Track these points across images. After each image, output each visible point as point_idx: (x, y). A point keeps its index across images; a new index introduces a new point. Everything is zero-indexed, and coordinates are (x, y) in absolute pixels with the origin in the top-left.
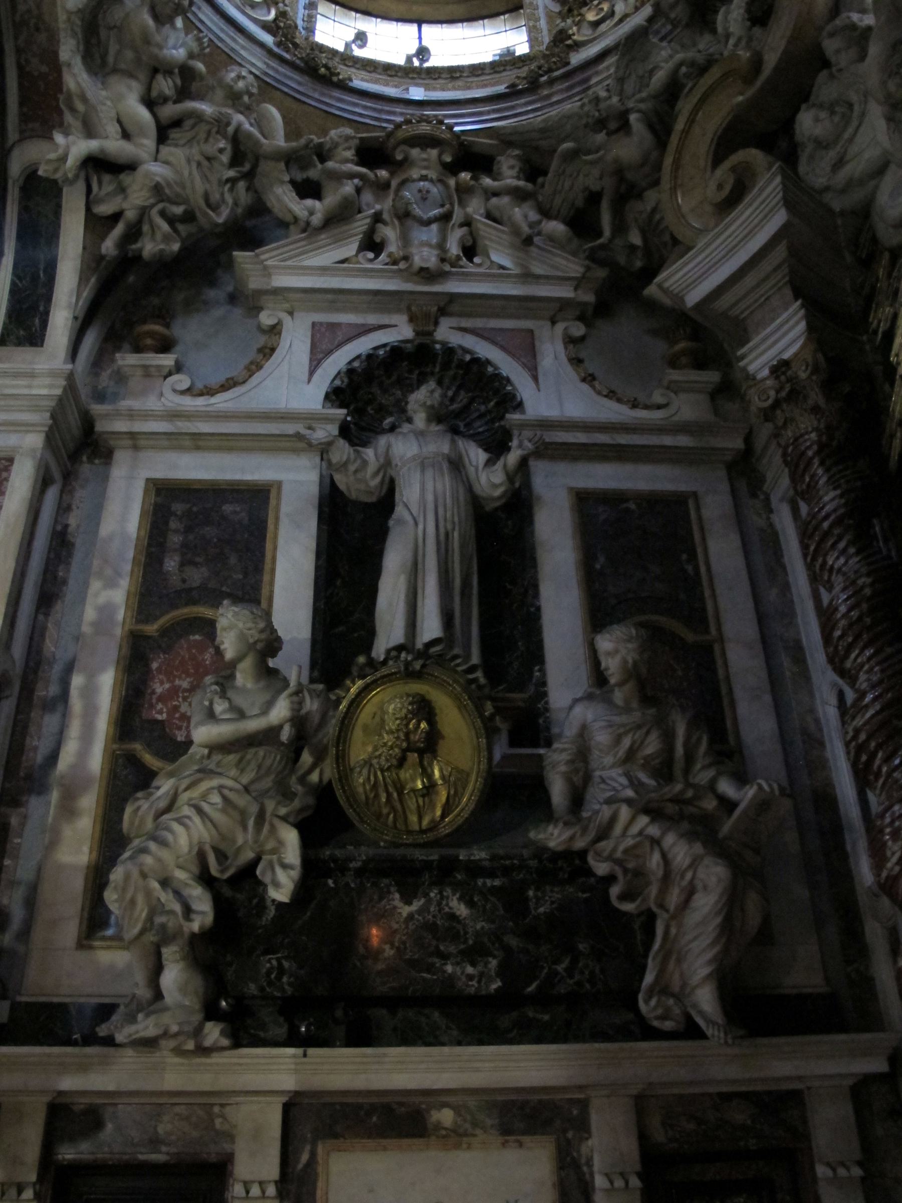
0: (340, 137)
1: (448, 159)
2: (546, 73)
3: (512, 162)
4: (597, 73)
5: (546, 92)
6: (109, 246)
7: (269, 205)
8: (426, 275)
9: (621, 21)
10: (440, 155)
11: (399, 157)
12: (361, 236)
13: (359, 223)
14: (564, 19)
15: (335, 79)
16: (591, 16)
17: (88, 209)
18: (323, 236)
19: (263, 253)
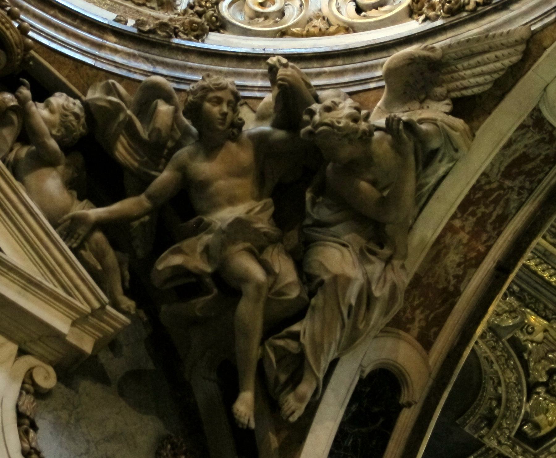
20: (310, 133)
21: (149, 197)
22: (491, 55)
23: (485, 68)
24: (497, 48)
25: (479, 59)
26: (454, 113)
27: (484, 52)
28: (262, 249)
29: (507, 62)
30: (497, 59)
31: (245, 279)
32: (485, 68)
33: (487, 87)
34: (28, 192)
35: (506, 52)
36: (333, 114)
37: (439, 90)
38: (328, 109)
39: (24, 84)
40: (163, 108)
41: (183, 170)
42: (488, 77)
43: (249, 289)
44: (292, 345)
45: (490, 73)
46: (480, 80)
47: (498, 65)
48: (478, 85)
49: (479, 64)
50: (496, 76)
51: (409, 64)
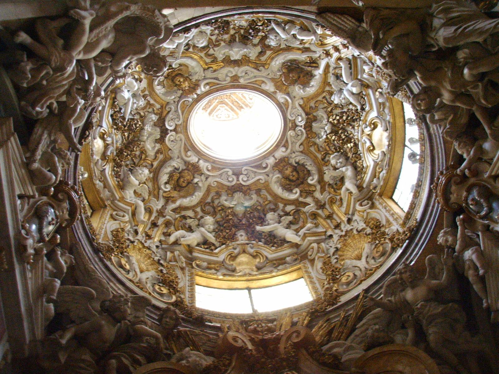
0: (69, 159)
1: (63, 225)
2: (103, 254)
3: (69, 261)
4: (115, 284)
5: (97, 259)
6: (24, 37)
7: (36, 130)
8: (22, 248)
9: (127, 278)
10: (66, 220)
11: (60, 196)
12: (23, 193)
13: (30, 189)
14: (114, 245)
15: (83, 141)
16: (123, 261)
17: (38, 18)
18: (23, 171)
19: (15, 139)
20: (403, 76)
21: (472, 107)
22: (334, 22)
23: (341, 22)
24: (330, 22)
25: (339, 25)
26: (363, 21)
27: (335, 25)
28: (460, 67)
29: (332, 16)
30: (334, 20)
31: (471, 75)
32: (341, 22)
33: (346, 16)
34: (494, 157)
35: (329, 19)
36: (390, 74)
37: (360, 29)
38: (390, 76)
39: (456, 173)
40: (436, 117)
41: (453, 101)
42: (342, 18)
43: (475, 72)
44: (489, 42)
45: (340, 19)
46: (345, 20)
47: (335, 18)
48: (348, 20)
49: (341, 24)
50: (340, 16)
51: (360, 46)
